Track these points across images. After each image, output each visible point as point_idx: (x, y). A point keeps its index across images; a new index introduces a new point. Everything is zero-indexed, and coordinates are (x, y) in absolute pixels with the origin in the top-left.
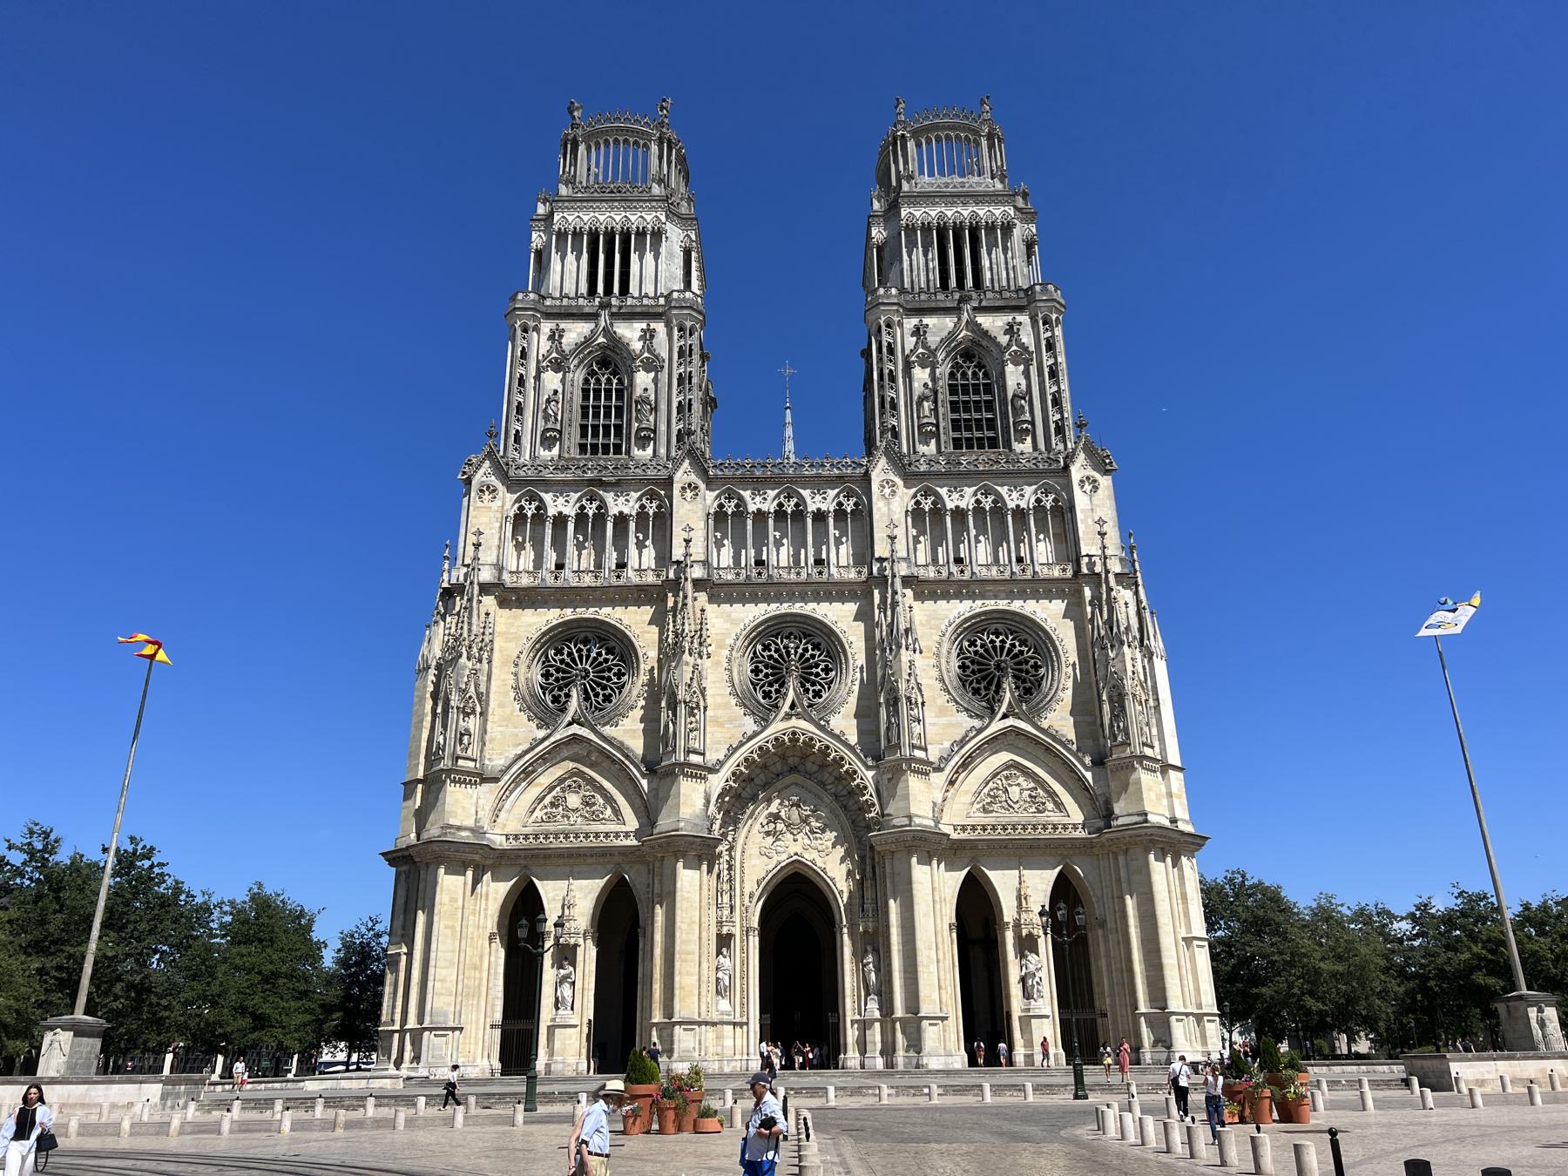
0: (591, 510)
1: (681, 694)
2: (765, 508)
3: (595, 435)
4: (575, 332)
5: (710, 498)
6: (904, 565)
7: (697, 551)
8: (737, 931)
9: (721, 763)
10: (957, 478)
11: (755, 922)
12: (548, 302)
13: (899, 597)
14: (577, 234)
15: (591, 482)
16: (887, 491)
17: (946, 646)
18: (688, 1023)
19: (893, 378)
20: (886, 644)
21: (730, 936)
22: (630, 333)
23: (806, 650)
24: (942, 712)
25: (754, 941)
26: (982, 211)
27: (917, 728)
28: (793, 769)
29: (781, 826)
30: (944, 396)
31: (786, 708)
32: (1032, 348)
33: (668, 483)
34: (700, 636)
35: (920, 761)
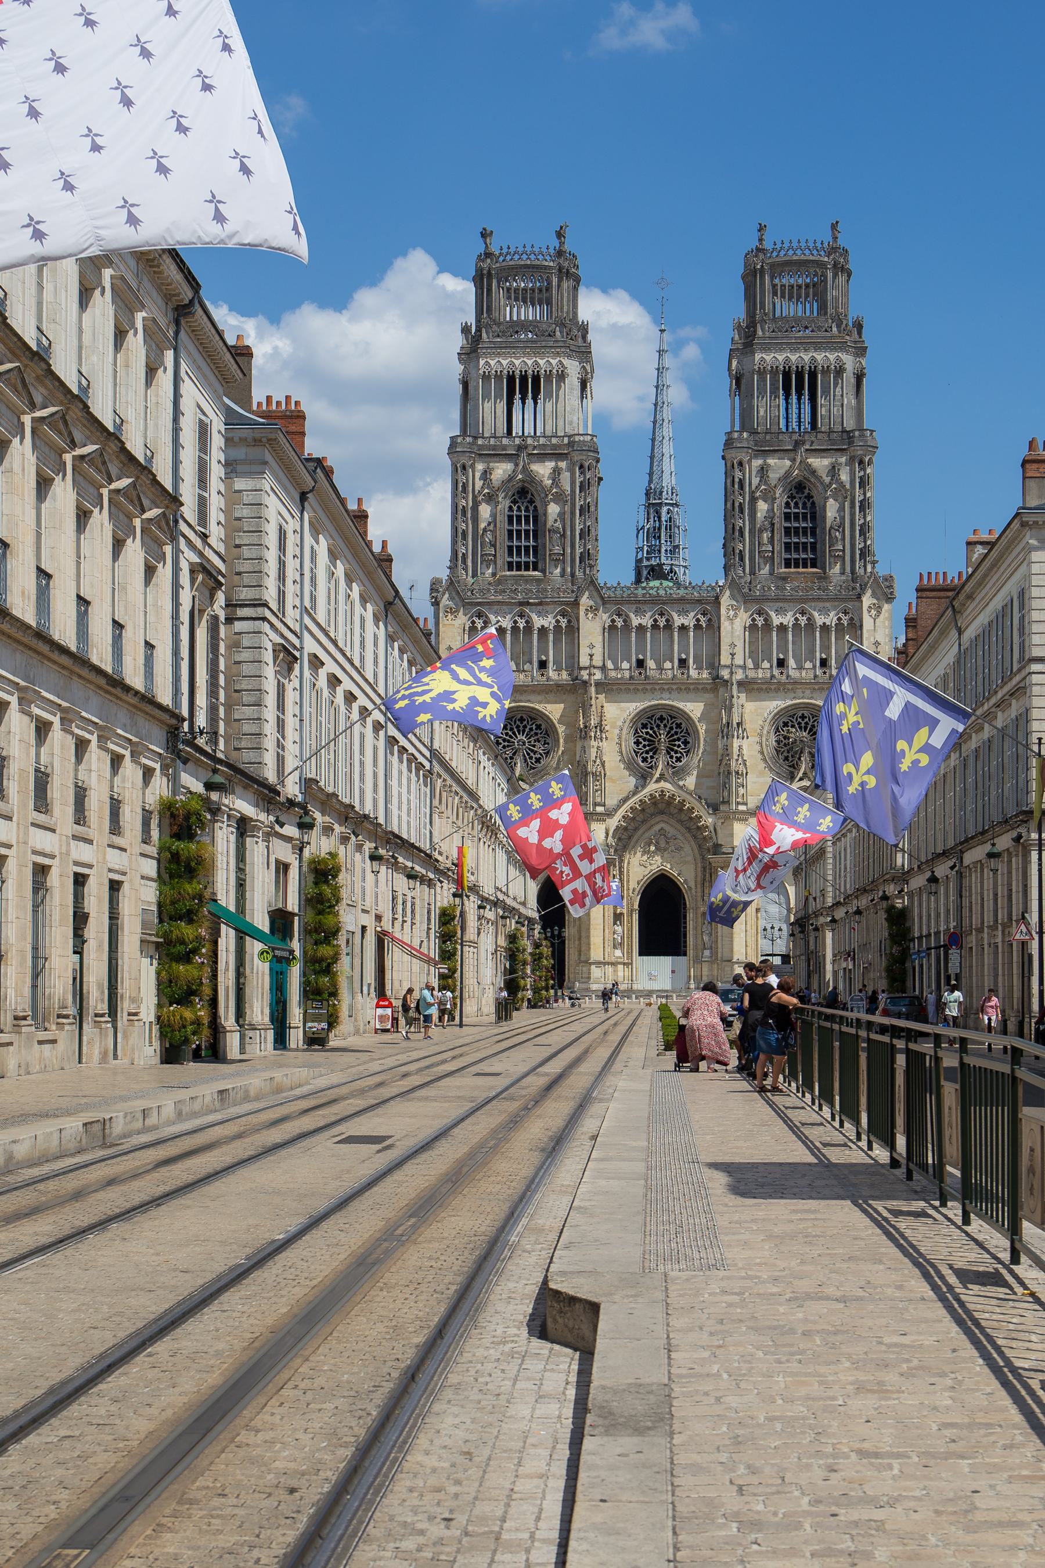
0: (521, 624)
1: (590, 768)
2: (644, 622)
3: (519, 554)
4: (501, 470)
5: (605, 617)
6: (740, 671)
7: (598, 661)
8: (625, 911)
9: (616, 810)
10: (782, 601)
11: (636, 906)
12: (480, 442)
13: (735, 700)
14: (498, 377)
15: (521, 604)
16: (732, 613)
17: (766, 729)
18: (598, 963)
19: (742, 511)
20: (726, 730)
21: (621, 914)
22: (543, 470)
23: (671, 728)
24: (761, 774)
25: (636, 917)
26: (819, 357)
27: (741, 791)
28: (662, 813)
29: (653, 848)
30: (780, 523)
31: (657, 775)
32: (848, 487)
33: (576, 604)
34: (600, 726)
35: (743, 812)
